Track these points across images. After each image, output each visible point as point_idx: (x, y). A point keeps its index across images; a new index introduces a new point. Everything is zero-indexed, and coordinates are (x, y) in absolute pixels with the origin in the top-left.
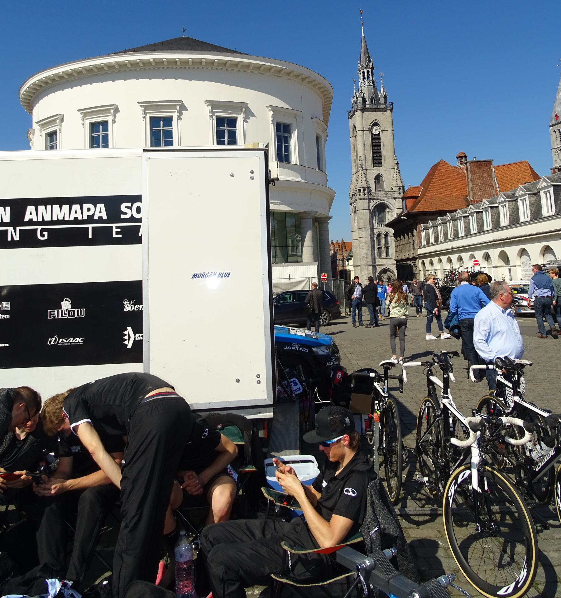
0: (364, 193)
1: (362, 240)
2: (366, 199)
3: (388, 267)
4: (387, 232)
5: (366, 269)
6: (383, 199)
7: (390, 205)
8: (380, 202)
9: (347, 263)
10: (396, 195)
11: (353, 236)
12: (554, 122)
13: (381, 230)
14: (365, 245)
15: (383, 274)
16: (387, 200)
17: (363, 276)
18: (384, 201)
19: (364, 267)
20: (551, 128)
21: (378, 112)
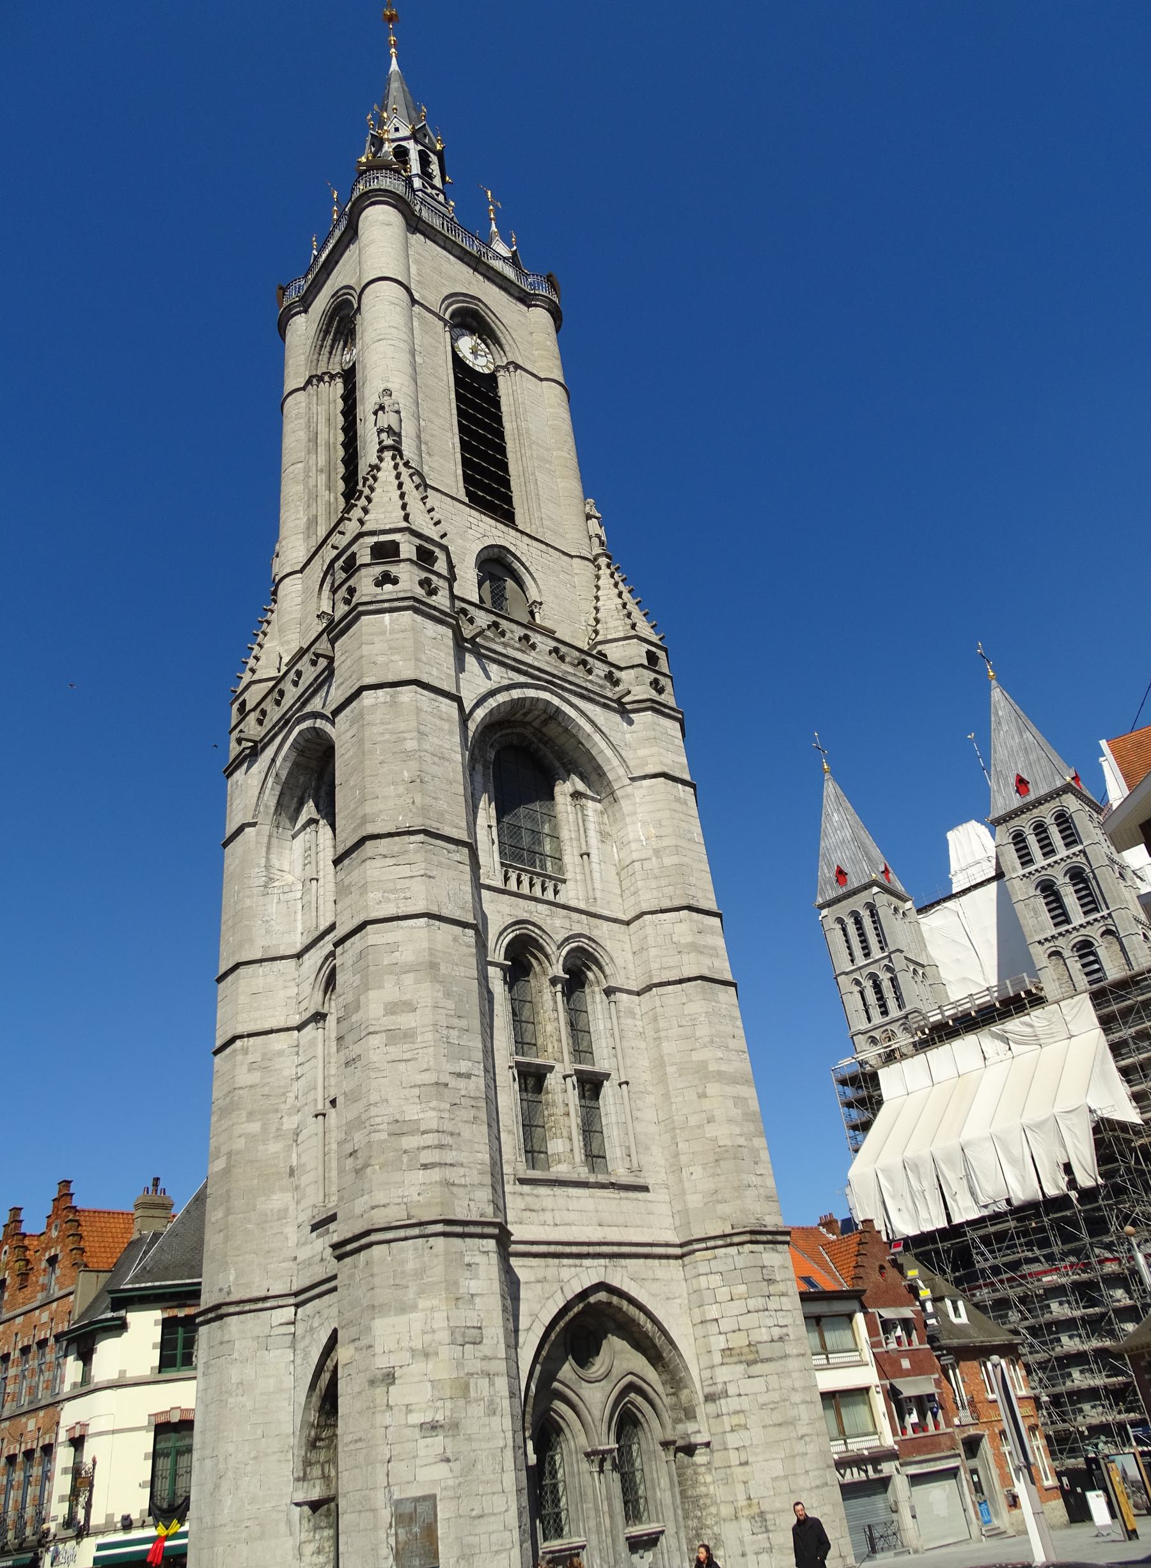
1: (394, 947)
2: (437, 617)
3: (620, 1276)
4: (584, 943)
5: (437, 1272)
6: (551, 682)
7: (597, 737)
8: (531, 693)
9: (72, 1368)
10: (636, 685)
11: (243, 999)
12: (831, 894)
13: (539, 913)
14: (424, 993)
15: (567, 1371)
17: (390, 1378)
18: (556, 701)
19: (409, 1253)
20: (824, 912)
21: (489, 279)
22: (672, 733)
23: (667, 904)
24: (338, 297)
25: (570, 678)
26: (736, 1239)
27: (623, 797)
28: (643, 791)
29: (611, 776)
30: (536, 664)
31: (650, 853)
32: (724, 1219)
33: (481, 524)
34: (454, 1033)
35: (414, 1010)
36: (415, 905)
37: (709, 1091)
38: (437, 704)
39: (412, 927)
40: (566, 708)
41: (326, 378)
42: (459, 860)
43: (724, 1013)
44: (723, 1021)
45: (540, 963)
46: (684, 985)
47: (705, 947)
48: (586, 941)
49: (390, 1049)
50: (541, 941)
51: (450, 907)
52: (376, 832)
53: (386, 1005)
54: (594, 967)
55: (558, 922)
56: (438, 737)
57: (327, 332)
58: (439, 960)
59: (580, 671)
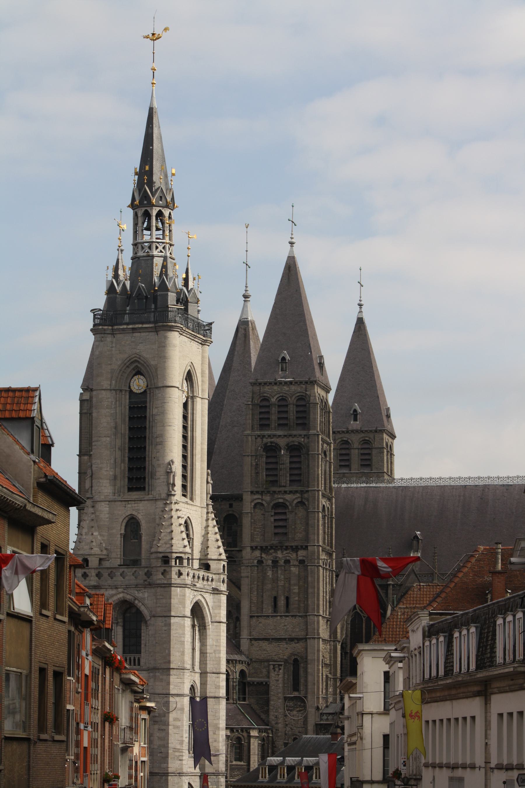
23: (215, 671)
24: (140, 358)
26: (216, 774)
29: (206, 621)
31: (212, 651)
32: (214, 769)
35: (180, 721)
37: (216, 733)
41: (123, 393)
52: (174, 667)
57: (128, 367)
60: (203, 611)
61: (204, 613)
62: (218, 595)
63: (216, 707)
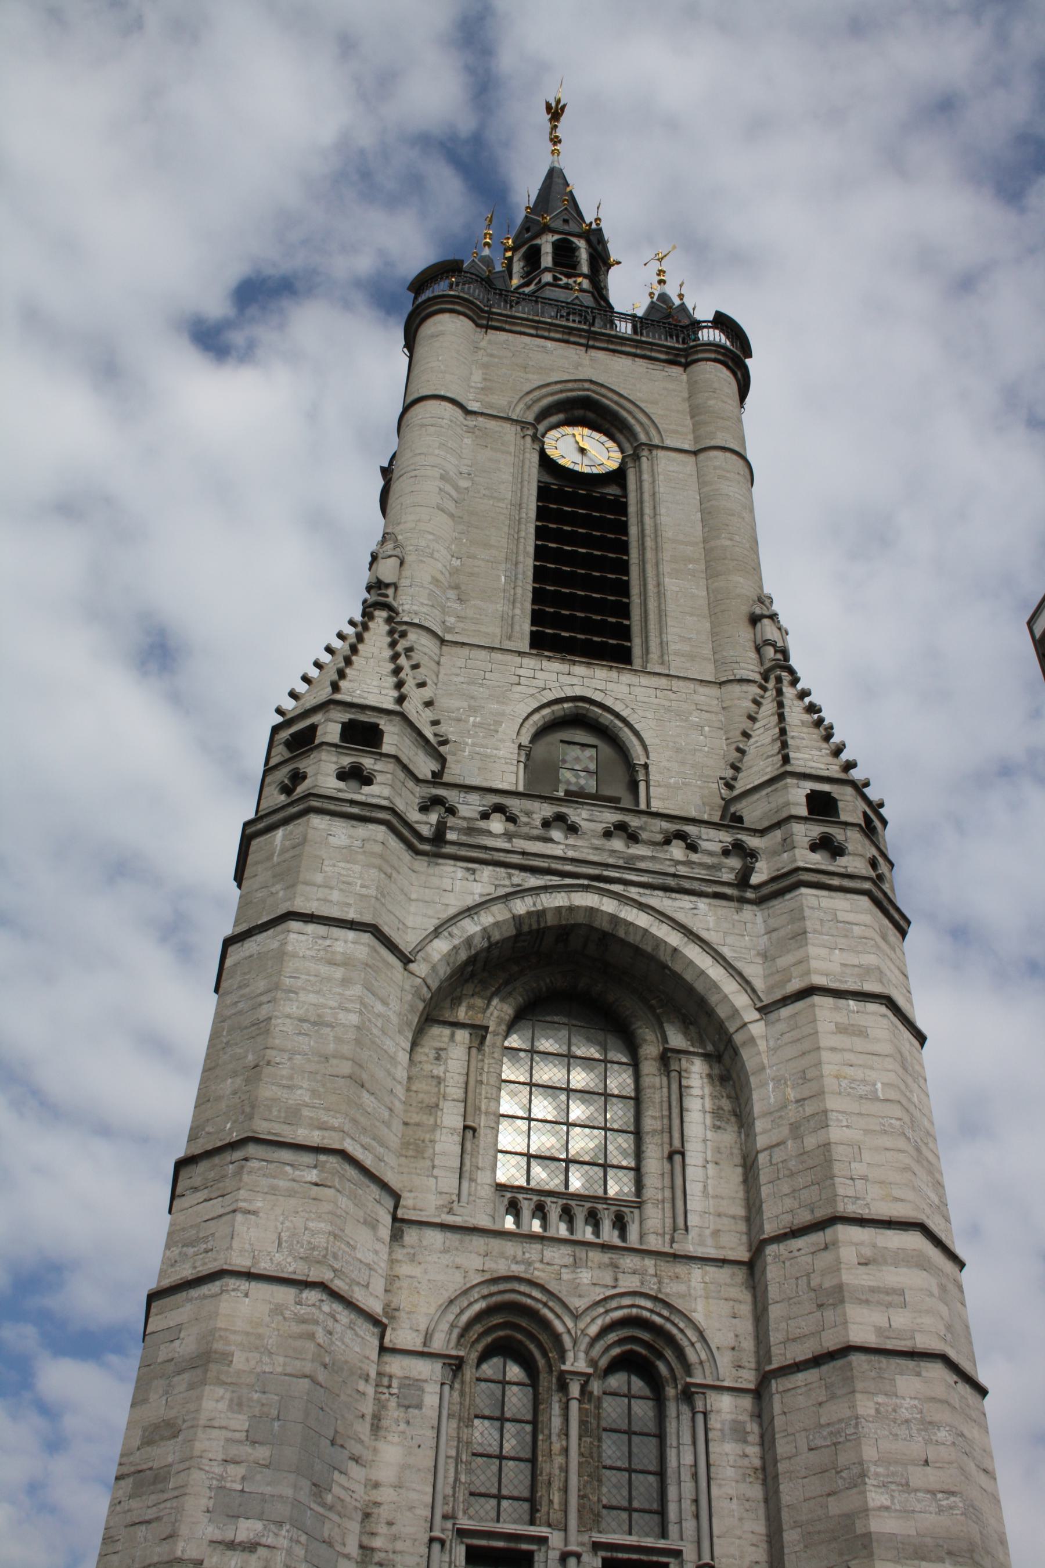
0: (346, 761)
7: (693, 953)
8: (559, 900)
16: (658, 900)
18: (609, 906)
22: (851, 917)
23: (805, 1217)
25: (642, 865)
27: (744, 1043)
28: (781, 1026)
30: (571, 854)
31: (785, 1131)
33: (539, 674)
34: (236, 1471)
36: (215, 1260)
38: (328, 942)
39: (205, 1297)
40: (630, 914)
42: (315, 1179)
43: (907, 1415)
44: (903, 1432)
45: (545, 1354)
46: (824, 1368)
47: (873, 1290)
48: (649, 1304)
49: (134, 1504)
50: (546, 1312)
51: (278, 1257)
53: (145, 1430)
54: (669, 1354)
55: (585, 1276)
56: (318, 992)
58: (233, 1348)
59: (677, 851)
60: (677, 968)
61: (688, 977)
62: (788, 896)
63: (836, 1411)
